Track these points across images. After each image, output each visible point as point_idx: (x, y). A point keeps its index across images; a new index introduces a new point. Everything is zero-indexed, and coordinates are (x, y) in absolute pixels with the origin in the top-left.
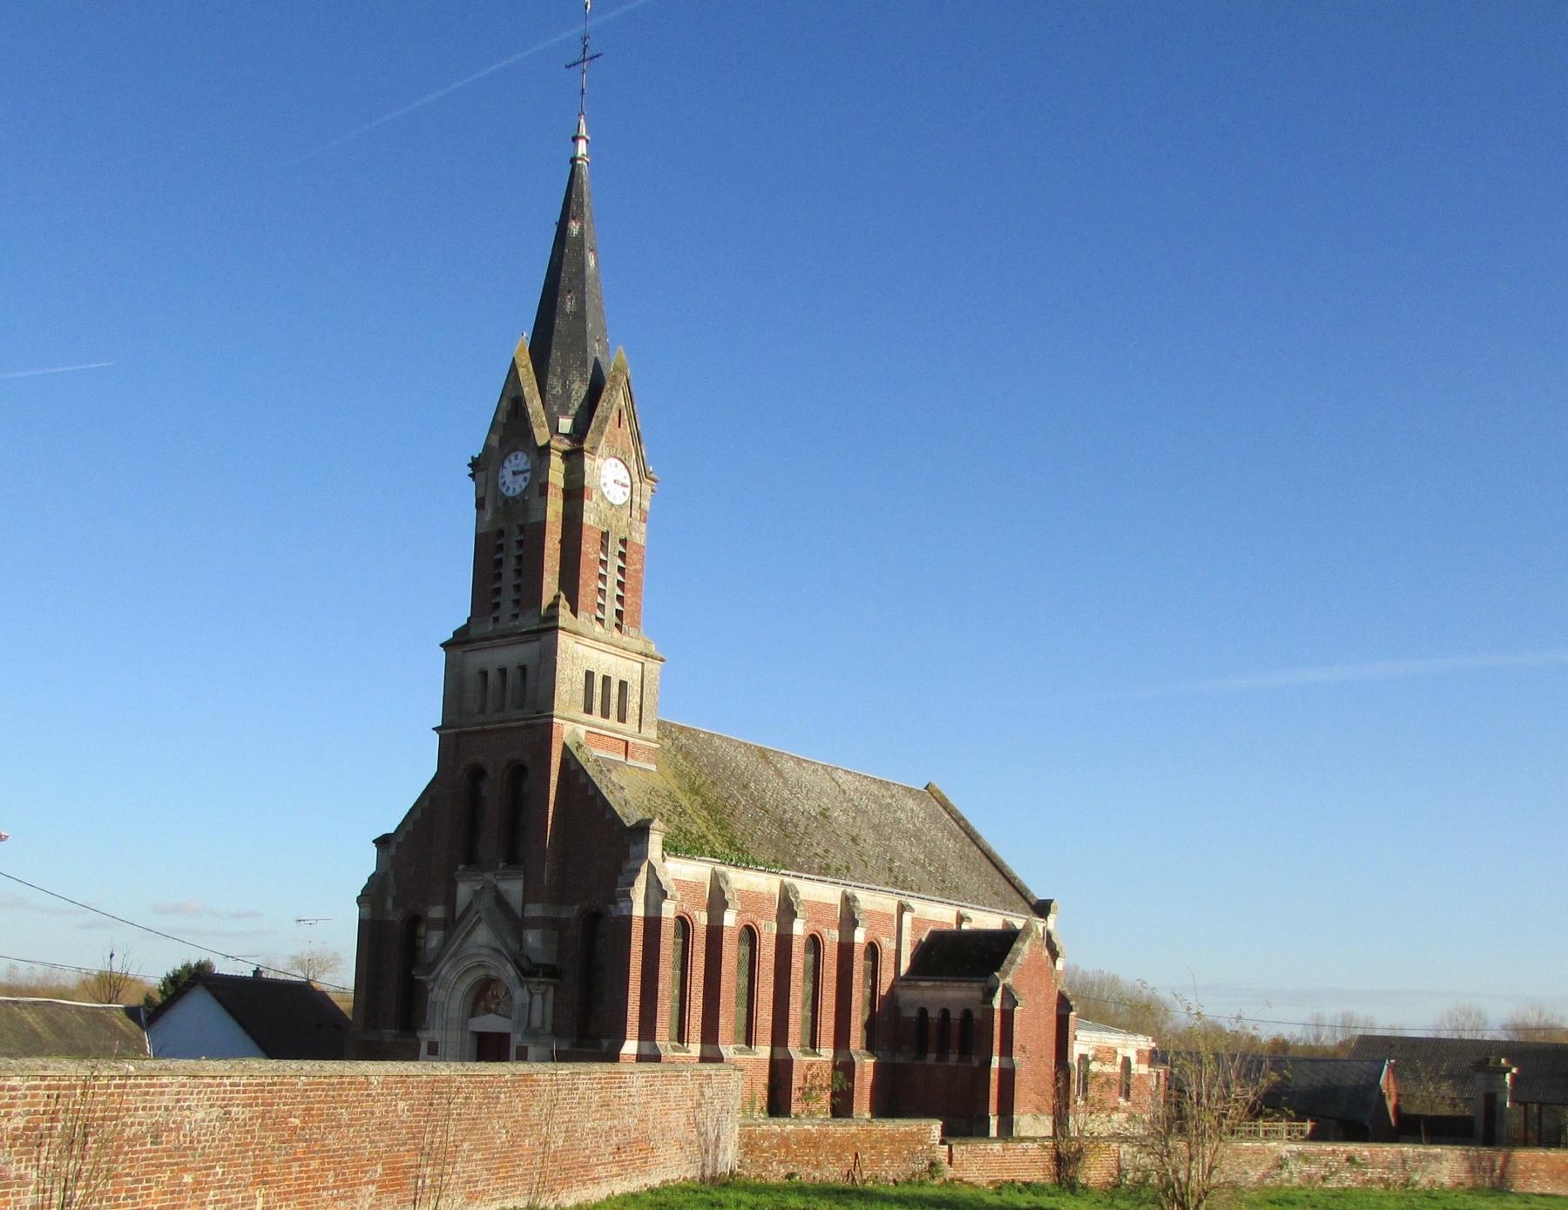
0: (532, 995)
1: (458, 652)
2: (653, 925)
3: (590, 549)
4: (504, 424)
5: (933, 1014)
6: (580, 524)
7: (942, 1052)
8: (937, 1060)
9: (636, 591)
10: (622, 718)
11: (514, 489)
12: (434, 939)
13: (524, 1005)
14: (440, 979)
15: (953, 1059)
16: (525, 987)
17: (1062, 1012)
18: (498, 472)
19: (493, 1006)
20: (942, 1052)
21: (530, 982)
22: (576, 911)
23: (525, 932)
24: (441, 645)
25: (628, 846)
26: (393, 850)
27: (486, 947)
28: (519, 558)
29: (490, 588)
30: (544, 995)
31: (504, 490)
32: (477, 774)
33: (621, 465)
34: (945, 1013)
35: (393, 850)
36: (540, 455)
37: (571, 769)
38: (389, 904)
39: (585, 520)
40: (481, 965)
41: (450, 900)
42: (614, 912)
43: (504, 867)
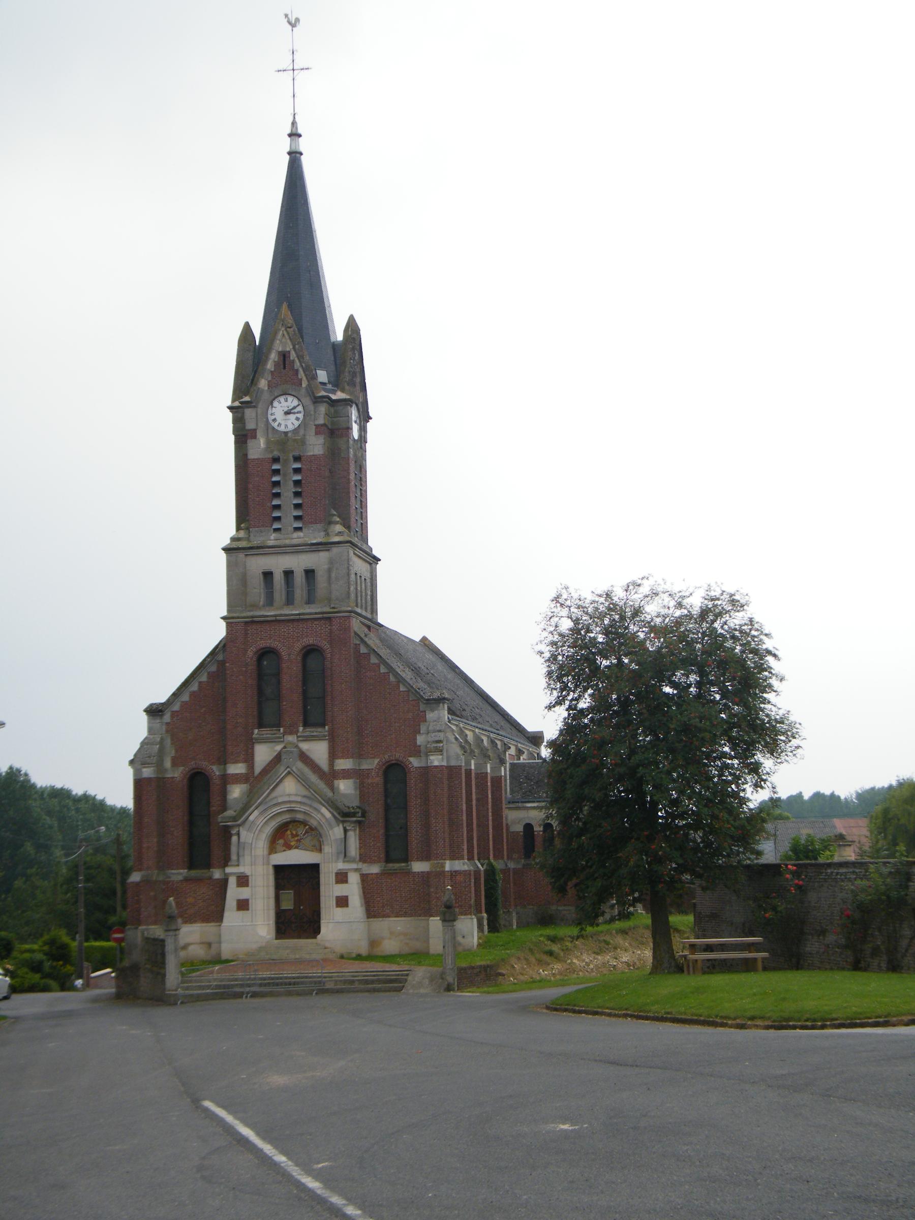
0: (346, 831)
1: (241, 555)
11: (286, 426)
12: (236, 792)
14: (247, 825)
16: (341, 826)
19: (292, 844)
23: (336, 782)
26: (167, 718)
27: (296, 795)
29: (269, 504)
31: (275, 425)
38: (168, 764)
41: (249, 759)
42: (415, 762)
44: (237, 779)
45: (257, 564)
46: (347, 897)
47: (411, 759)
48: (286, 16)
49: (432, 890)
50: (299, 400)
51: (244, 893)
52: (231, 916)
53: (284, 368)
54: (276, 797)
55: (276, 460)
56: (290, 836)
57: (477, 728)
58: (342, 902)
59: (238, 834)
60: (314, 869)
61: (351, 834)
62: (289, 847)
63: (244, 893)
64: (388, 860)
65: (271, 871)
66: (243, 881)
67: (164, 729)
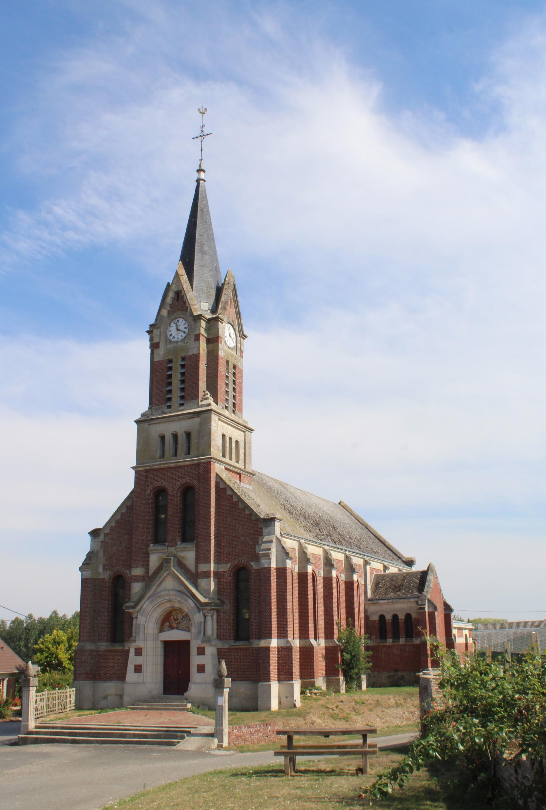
0: (205, 617)
1: (146, 425)
2: (282, 572)
3: (222, 369)
4: (170, 305)
5: (389, 617)
6: (217, 356)
7: (396, 637)
8: (393, 642)
9: (241, 393)
10: (237, 462)
11: (178, 338)
12: (136, 588)
13: (201, 623)
14: (141, 612)
15: (402, 641)
16: (201, 612)
17: (447, 612)
18: (167, 329)
19: (175, 625)
20: (396, 637)
21: (204, 609)
22: (229, 567)
24: (135, 421)
25: (262, 528)
26: (102, 537)
28: (183, 374)
29: (165, 390)
30: (212, 616)
31: (171, 338)
32: (160, 492)
33: (231, 328)
34: (395, 617)
35: (102, 537)
36: (194, 320)
37: (221, 487)
38: (101, 569)
39: (220, 354)
40: (170, 601)
41: (146, 564)
42: (254, 565)
43: (180, 544)
44: (137, 579)
45: (156, 430)
46: (204, 665)
47: (252, 563)
48: (199, 110)
49: (261, 661)
50: (186, 320)
51: (139, 660)
52: (131, 675)
53: (178, 301)
54: (160, 592)
55: (170, 361)
56: (173, 620)
57: (325, 545)
58: (201, 669)
59: (137, 618)
60: (187, 643)
61: (209, 619)
62: (171, 628)
63: (139, 660)
64: (237, 638)
65: (160, 646)
66: (139, 652)
67: (100, 545)
